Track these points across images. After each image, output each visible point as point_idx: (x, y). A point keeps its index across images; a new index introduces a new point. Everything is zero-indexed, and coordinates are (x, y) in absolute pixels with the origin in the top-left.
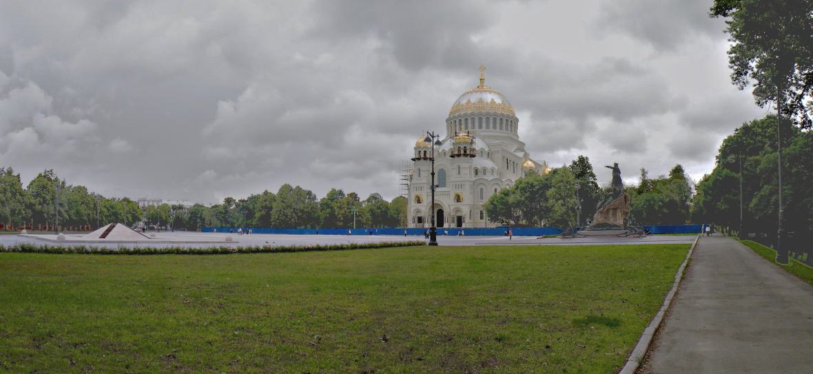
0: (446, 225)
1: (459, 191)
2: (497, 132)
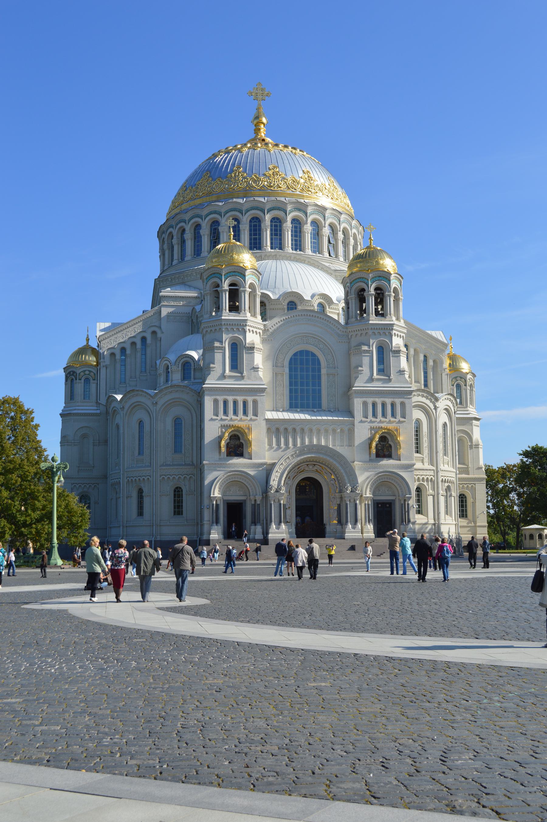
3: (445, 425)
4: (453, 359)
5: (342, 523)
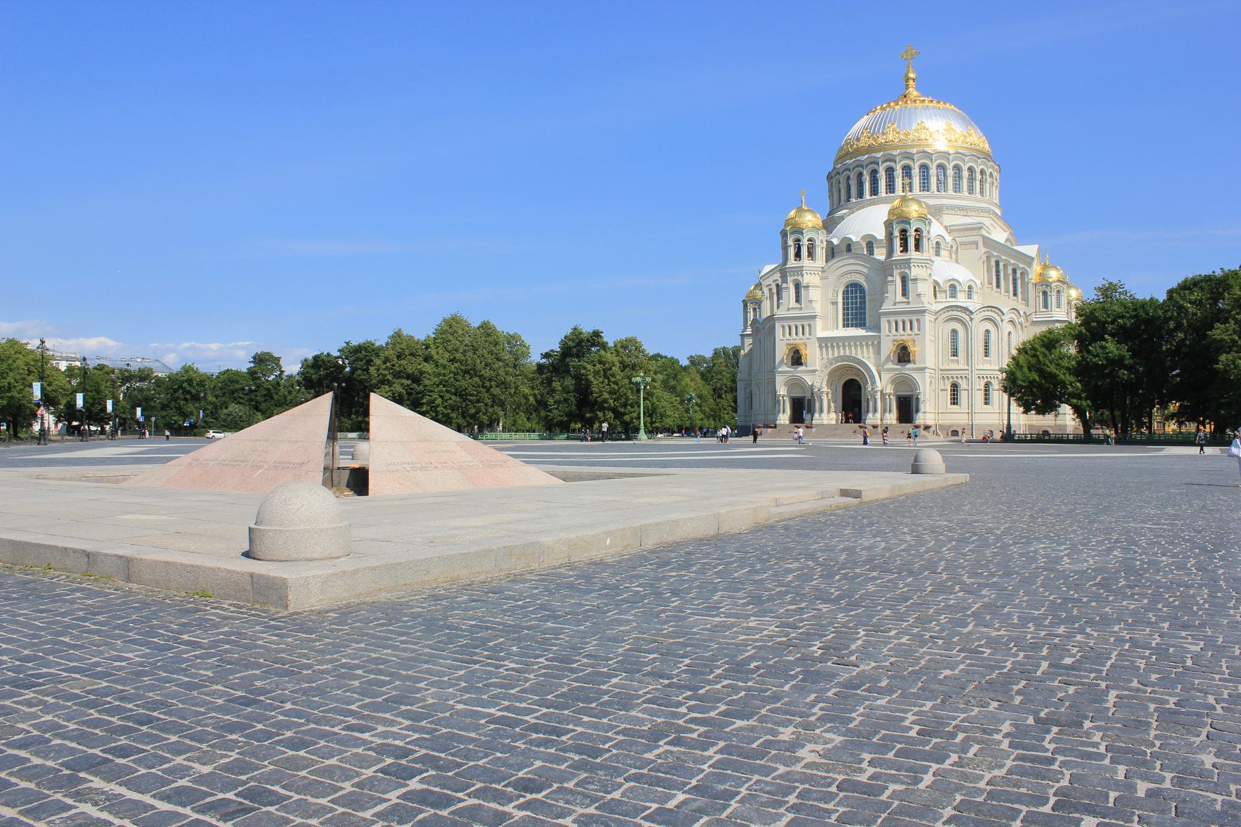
0: (871, 419)
1: (904, 336)
2: (964, 199)
3: (988, 331)
4: (1045, 267)
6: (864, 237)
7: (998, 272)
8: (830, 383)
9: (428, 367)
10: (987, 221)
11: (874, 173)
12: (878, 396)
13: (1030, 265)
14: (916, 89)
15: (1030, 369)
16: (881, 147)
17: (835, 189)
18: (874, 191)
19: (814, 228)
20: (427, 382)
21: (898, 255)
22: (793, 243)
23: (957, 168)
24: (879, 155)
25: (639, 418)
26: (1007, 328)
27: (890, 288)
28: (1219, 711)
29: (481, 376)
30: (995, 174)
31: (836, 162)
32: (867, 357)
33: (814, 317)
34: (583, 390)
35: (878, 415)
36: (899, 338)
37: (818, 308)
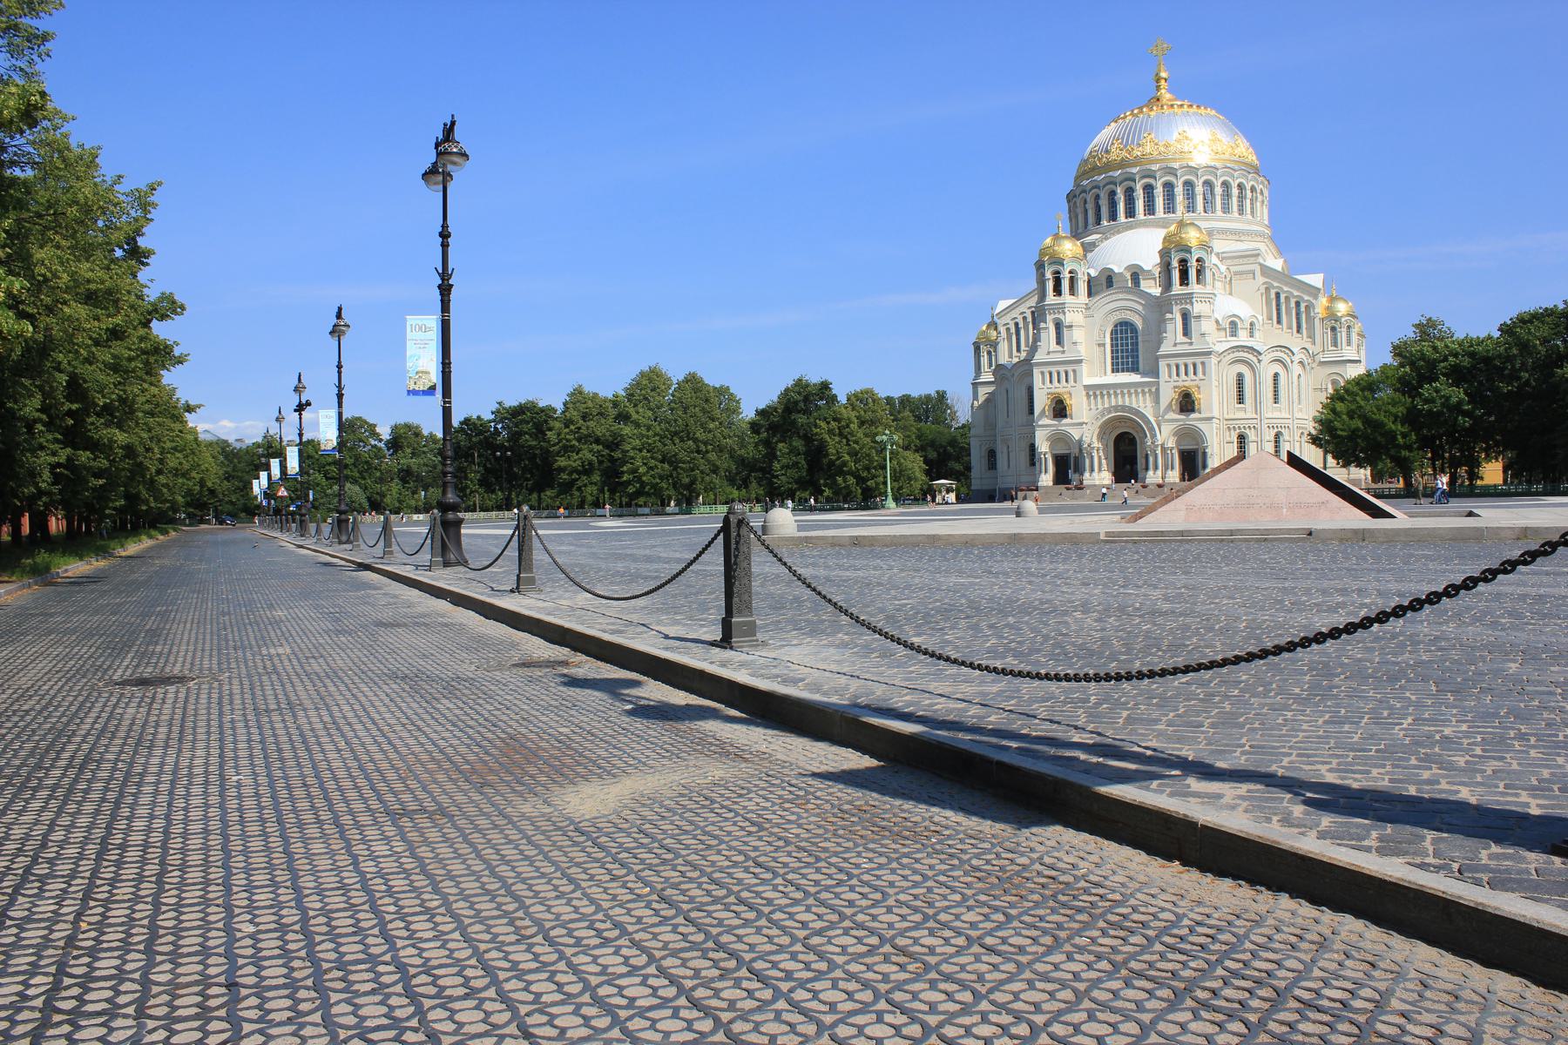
0: (1153, 477)
1: (1187, 382)
3: (1276, 376)
4: (1332, 299)
5: (1147, 469)
6: (1128, 268)
7: (1278, 305)
8: (1101, 437)
9: (627, 430)
10: (1262, 247)
11: (1129, 193)
12: (1159, 451)
13: (1316, 297)
14: (1169, 91)
15: (1351, 418)
16: (1137, 161)
17: (1080, 210)
18: (1130, 212)
19: (1075, 258)
20: (628, 447)
21: (1177, 289)
22: (1051, 277)
23: (1225, 184)
24: (1134, 170)
25: (885, 483)
26: (1296, 369)
27: (1169, 327)
28: (1555, 788)
29: (696, 440)
30: (1266, 193)
31: (1078, 178)
32: (1145, 406)
33: (1080, 361)
34: (816, 453)
35: (1159, 472)
36: (1180, 384)
37: (1083, 351)
